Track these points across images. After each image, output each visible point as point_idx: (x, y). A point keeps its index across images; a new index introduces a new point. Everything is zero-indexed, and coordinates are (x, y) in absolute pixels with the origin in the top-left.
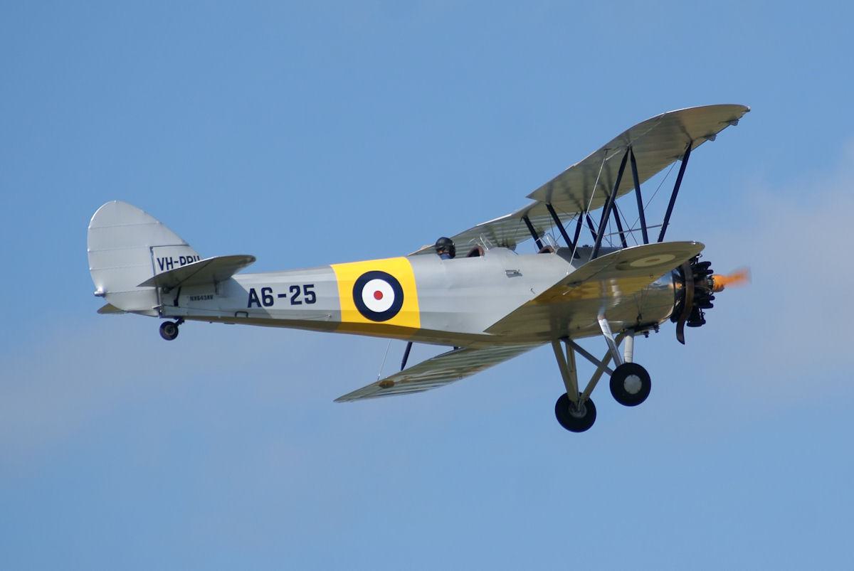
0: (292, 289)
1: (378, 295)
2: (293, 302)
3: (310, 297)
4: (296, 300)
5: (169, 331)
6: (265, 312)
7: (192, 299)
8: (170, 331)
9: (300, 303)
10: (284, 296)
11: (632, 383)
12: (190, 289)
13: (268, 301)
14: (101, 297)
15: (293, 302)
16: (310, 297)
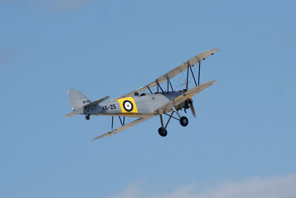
0: (111, 106)
1: (128, 106)
2: (112, 109)
3: (115, 107)
4: (112, 108)
5: (88, 118)
6: (106, 111)
7: (91, 110)
8: (88, 118)
9: (113, 109)
10: (109, 107)
11: (185, 121)
12: (91, 109)
13: (106, 109)
14: (73, 111)
15: (112, 109)
16: (115, 107)
